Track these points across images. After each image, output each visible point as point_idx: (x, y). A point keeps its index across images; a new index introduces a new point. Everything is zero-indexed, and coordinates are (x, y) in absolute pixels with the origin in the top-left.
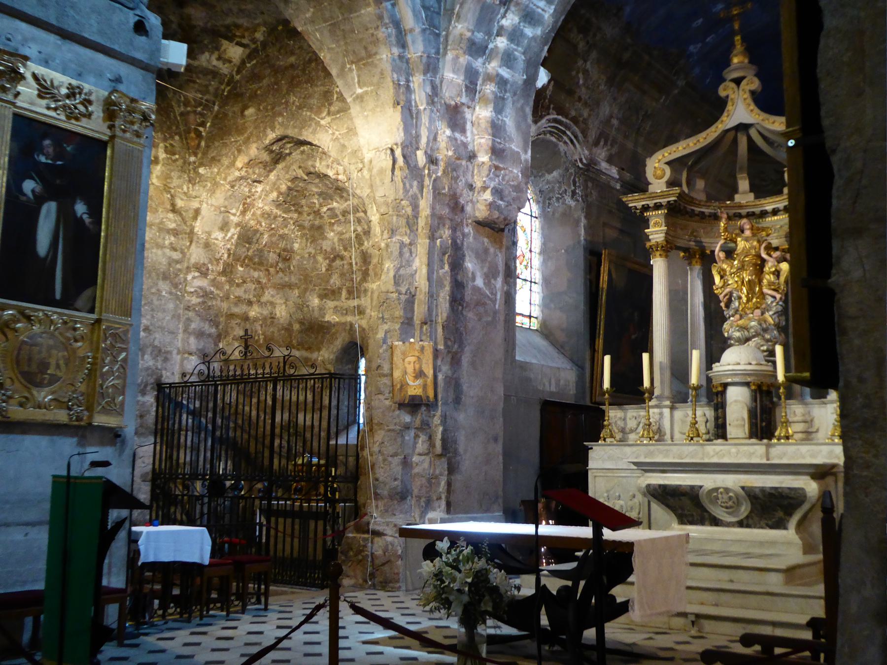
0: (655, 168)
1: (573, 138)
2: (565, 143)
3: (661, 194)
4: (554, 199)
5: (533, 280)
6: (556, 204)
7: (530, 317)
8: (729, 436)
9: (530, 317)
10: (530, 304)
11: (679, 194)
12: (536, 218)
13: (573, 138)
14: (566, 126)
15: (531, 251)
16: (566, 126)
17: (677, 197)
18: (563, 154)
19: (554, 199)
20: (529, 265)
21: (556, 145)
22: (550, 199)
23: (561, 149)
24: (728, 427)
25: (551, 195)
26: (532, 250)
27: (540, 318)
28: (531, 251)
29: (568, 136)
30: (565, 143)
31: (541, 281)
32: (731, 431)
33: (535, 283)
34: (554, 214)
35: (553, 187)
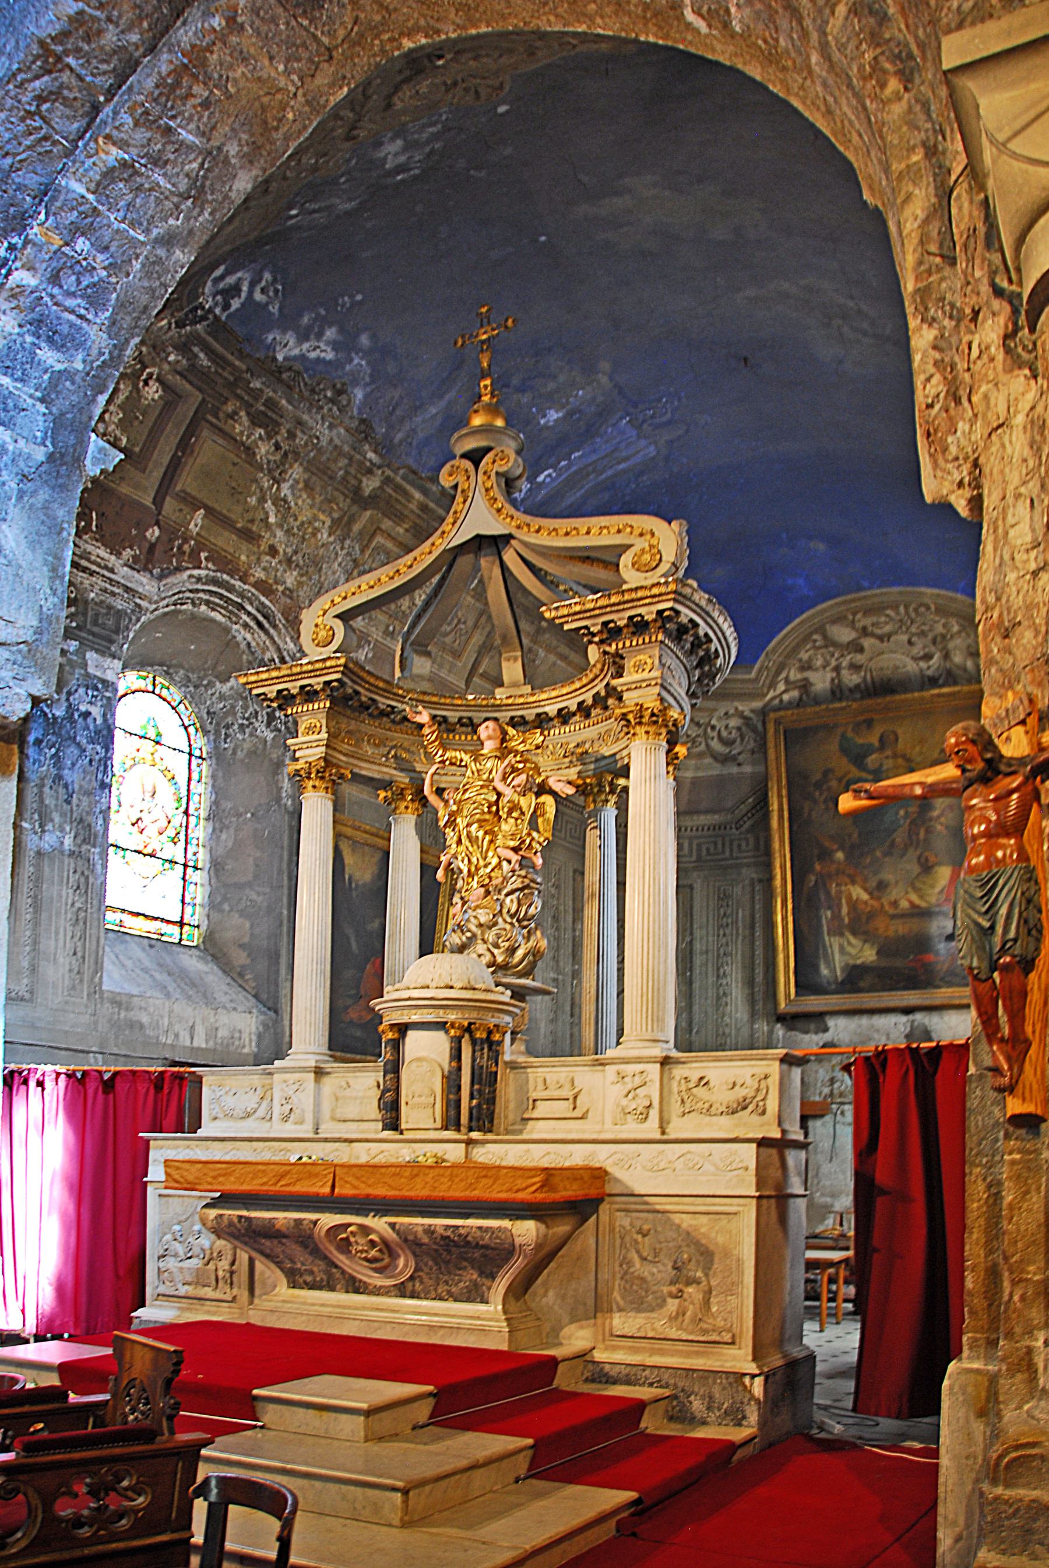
0: (317, 626)
1: (261, 618)
2: (246, 626)
3: (310, 667)
4: (236, 727)
5: (191, 863)
6: (240, 736)
7: (181, 924)
8: (403, 1126)
9: (181, 924)
10: (183, 902)
11: (345, 666)
12: (201, 757)
13: (261, 618)
14: (241, 595)
15: (186, 812)
16: (241, 595)
17: (343, 673)
18: (243, 646)
19: (236, 727)
20: (182, 836)
21: (227, 630)
22: (228, 727)
23: (239, 638)
24: (403, 1108)
25: (230, 720)
26: (191, 811)
27: (203, 928)
28: (186, 812)
29: (249, 614)
30: (246, 626)
31: (208, 866)
32: (408, 1117)
33: (196, 868)
34: (234, 753)
35: (233, 707)
